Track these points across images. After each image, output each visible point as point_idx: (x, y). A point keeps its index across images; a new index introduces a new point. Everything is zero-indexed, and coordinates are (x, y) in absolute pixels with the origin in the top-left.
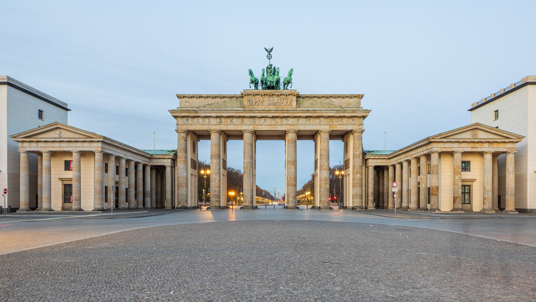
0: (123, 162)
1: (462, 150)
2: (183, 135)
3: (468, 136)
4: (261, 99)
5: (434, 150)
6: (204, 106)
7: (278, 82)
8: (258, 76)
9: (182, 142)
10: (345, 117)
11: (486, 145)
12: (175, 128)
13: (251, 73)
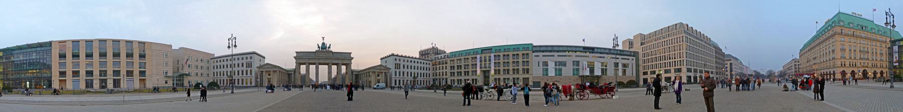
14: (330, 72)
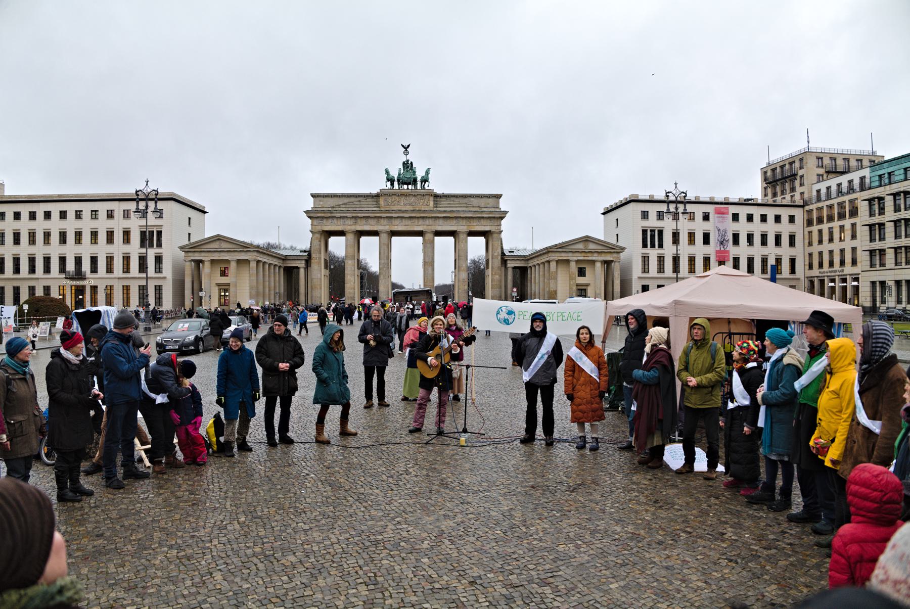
0: (267, 266)
1: (575, 258)
2: (318, 236)
3: (580, 246)
4: (397, 198)
5: (552, 258)
6: (339, 206)
7: (415, 180)
8: (394, 174)
9: (316, 242)
10: (483, 218)
11: (596, 255)
12: (310, 228)
13: (387, 172)
14: (429, 264)
